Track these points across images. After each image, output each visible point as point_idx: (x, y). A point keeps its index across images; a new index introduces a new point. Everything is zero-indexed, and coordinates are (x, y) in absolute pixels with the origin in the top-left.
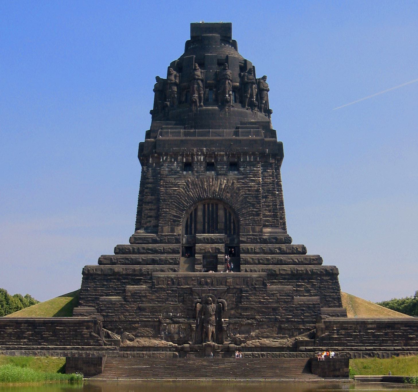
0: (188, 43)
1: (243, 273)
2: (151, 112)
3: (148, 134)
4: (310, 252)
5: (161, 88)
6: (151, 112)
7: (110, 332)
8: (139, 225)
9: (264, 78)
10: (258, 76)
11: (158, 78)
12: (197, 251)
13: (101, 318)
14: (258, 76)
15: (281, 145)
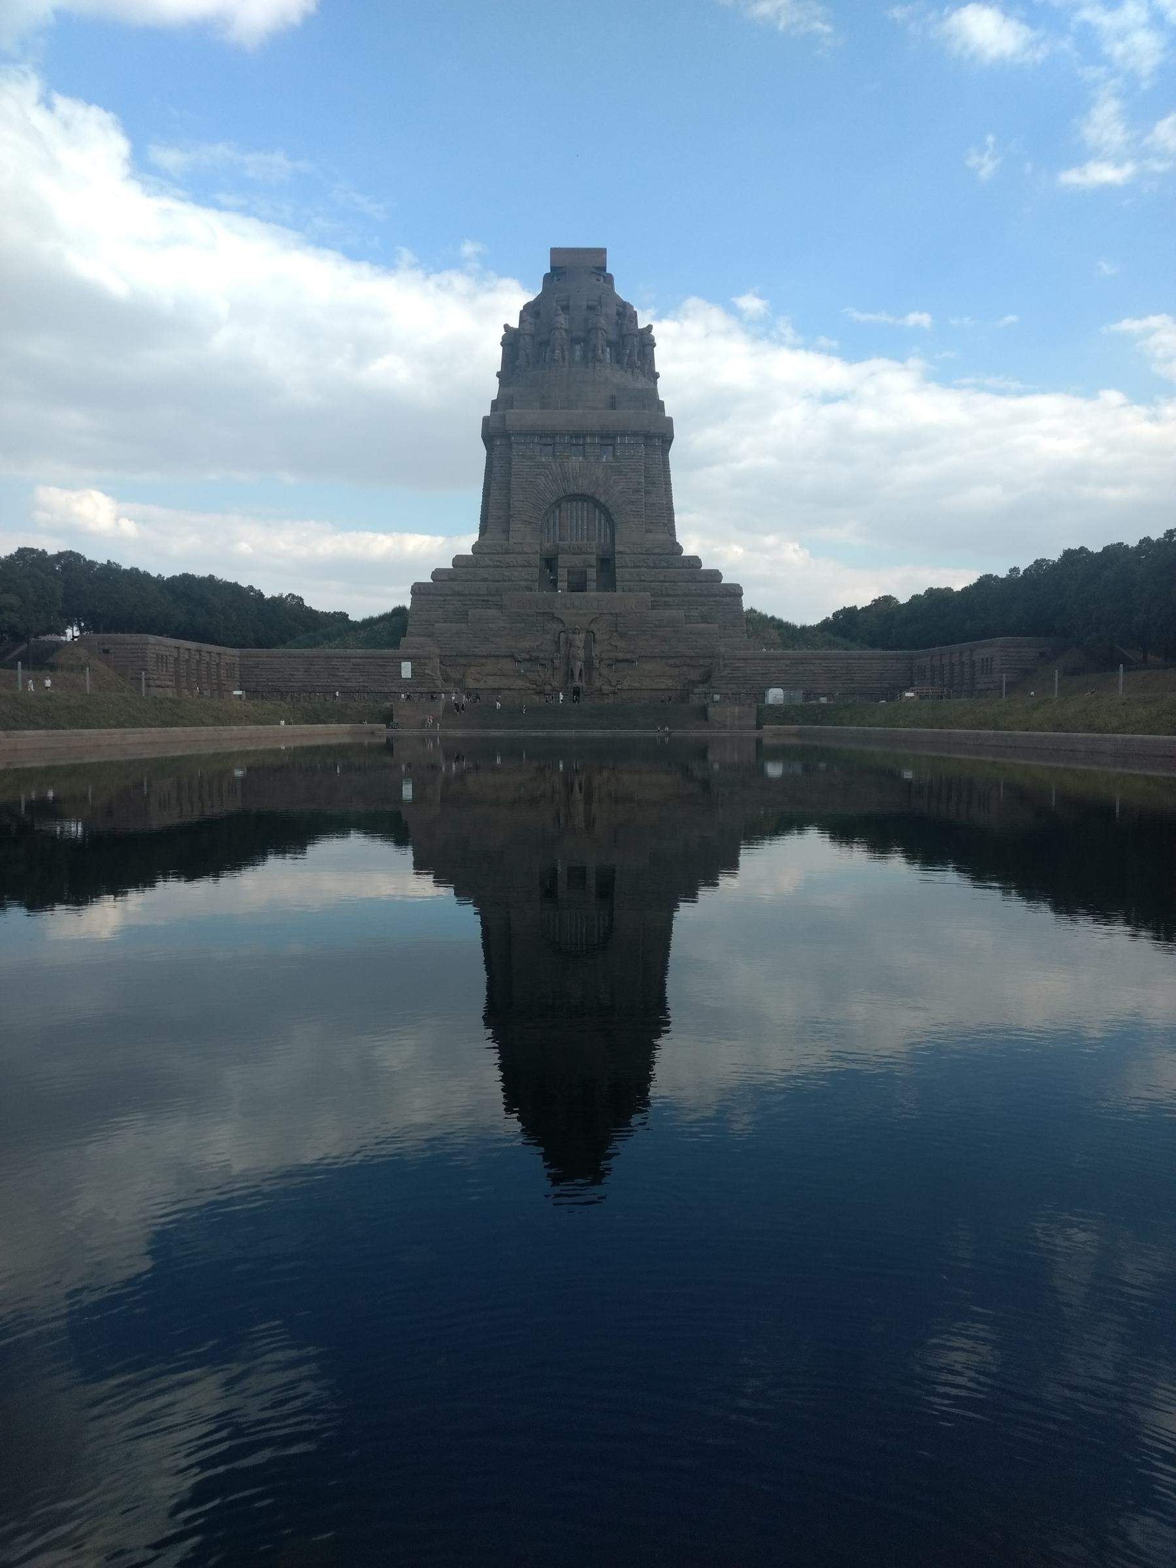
0: (547, 278)
1: (619, 593)
2: (498, 375)
3: (495, 405)
4: (705, 566)
5: (511, 340)
6: (498, 375)
7: (448, 669)
8: (483, 530)
9: (650, 327)
10: (642, 325)
11: (506, 327)
12: (560, 563)
13: (437, 651)
14: (642, 325)
15: (670, 421)
